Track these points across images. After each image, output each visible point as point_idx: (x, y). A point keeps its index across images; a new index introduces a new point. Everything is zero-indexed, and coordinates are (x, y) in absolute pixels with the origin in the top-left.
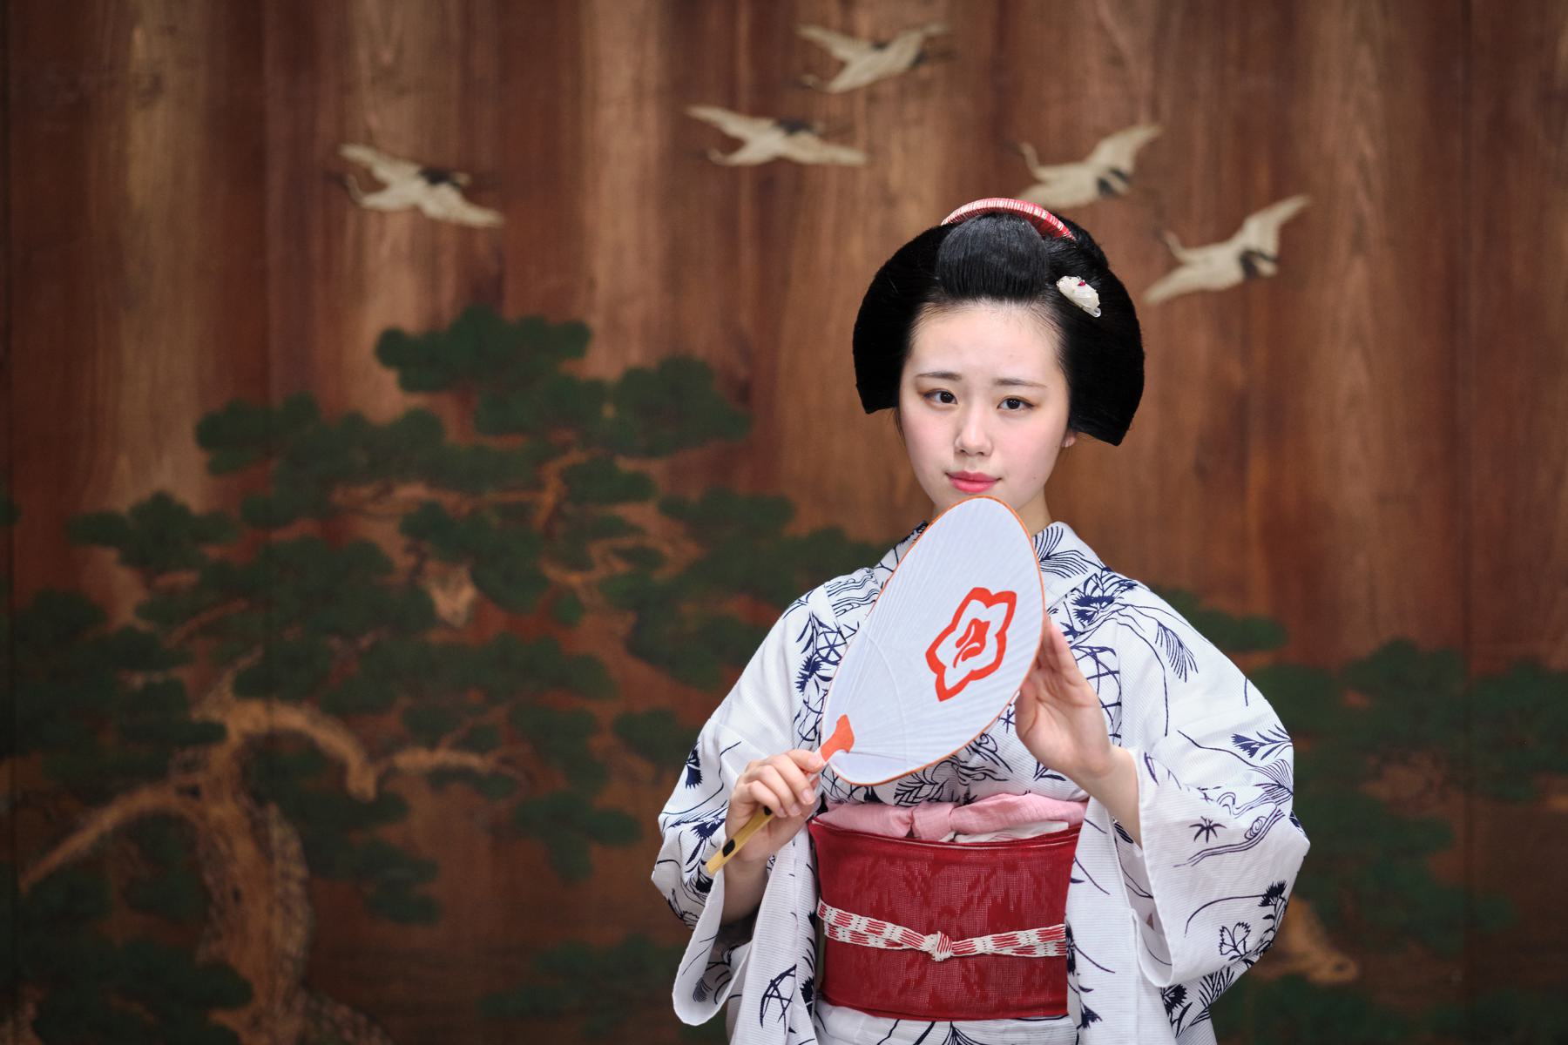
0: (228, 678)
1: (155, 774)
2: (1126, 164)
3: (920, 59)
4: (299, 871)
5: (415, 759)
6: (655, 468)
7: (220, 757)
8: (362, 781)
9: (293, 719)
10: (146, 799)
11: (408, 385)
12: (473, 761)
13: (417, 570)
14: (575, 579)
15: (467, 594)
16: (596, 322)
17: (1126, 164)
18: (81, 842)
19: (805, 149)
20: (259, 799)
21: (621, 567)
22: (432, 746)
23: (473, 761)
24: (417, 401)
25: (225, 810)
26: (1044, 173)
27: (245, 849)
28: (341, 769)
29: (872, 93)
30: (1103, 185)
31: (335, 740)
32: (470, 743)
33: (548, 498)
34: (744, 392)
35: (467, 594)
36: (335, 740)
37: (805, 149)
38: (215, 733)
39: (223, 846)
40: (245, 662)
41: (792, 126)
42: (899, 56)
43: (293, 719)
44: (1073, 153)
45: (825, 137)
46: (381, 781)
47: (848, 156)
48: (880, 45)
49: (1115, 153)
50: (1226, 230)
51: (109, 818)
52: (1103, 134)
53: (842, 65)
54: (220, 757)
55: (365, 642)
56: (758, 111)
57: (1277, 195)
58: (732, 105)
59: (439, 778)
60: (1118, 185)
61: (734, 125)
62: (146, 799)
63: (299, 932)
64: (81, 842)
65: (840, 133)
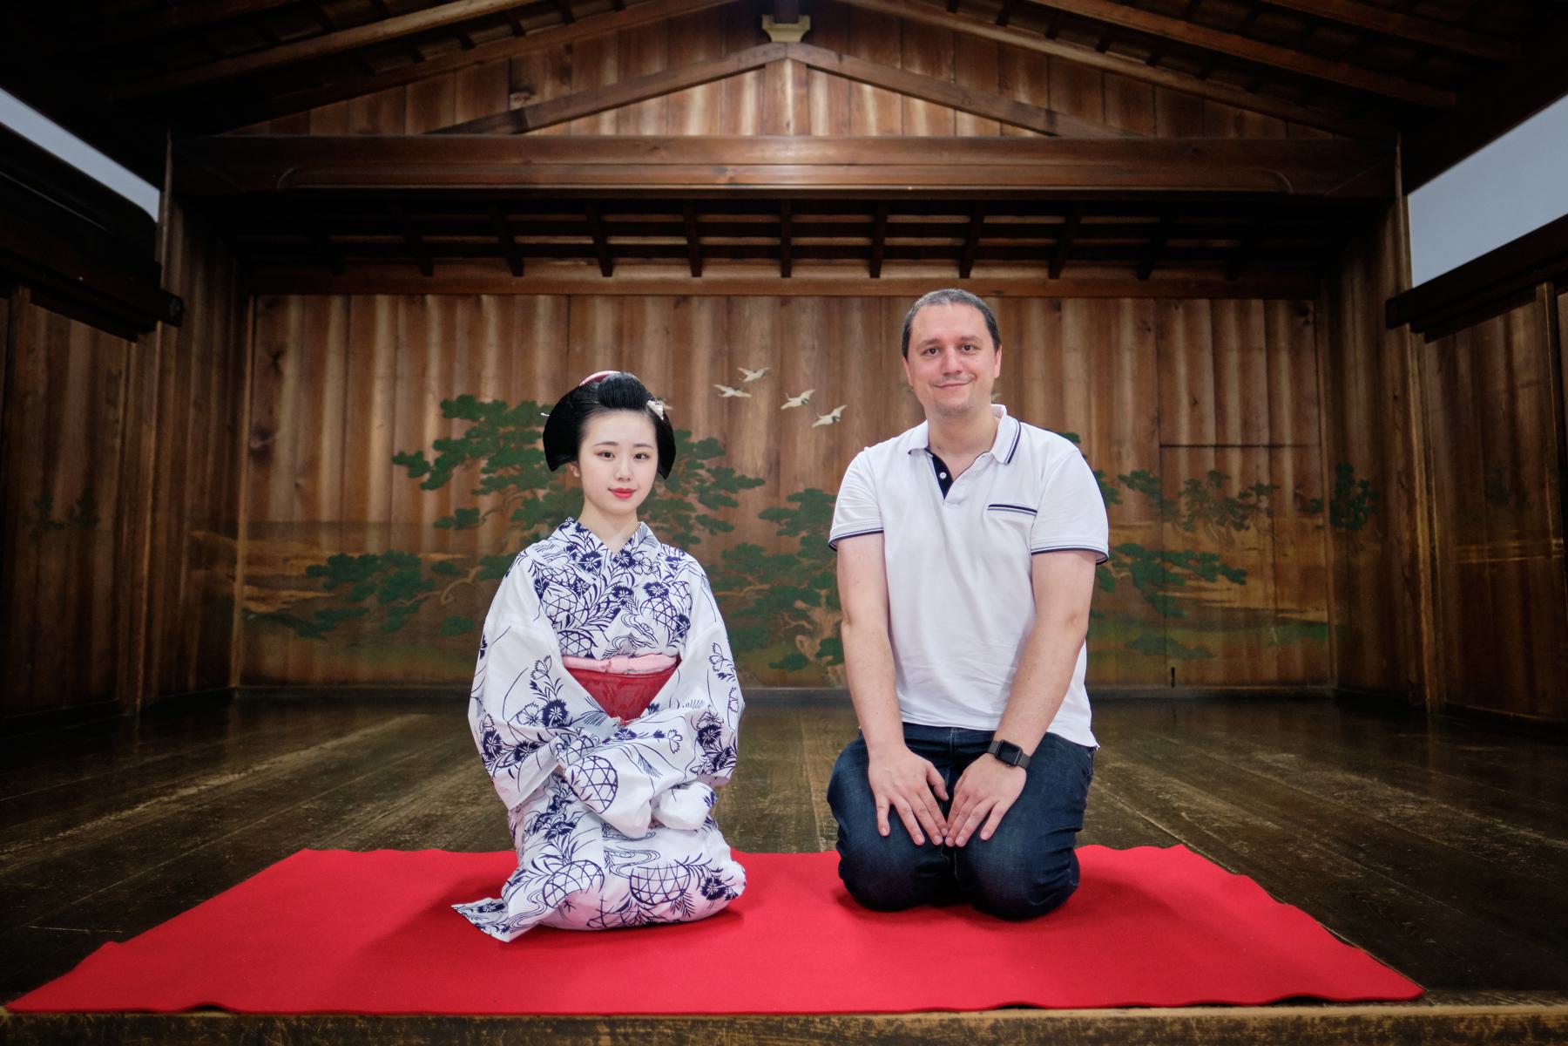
2: (807, 398)
3: (764, 375)
6: (705, 462)
12: (664, 525)
14: (687, 486)
16: (693, 431)
17: (807, 398)
19: (739, 394)
21: (697, 483)
23: (664, 525)
26: (790, 399)
29: (753, 382)
30: (803, 402)
34: (725, 446)
37: (739, 394)
41: (736, 389)
42: (759, 374)
44: (797, 395)
45: (743, 391)
47: (747, 395)
48: (755, 372)
49: (805, 395)
50: (829, 413)
52: (803, 391)
53: (746, 376)
56: (728, 386)
57: (840, 405)
58: (723, 384)
60: (806, 402)
61: (723, 388)
65: (746, 390)
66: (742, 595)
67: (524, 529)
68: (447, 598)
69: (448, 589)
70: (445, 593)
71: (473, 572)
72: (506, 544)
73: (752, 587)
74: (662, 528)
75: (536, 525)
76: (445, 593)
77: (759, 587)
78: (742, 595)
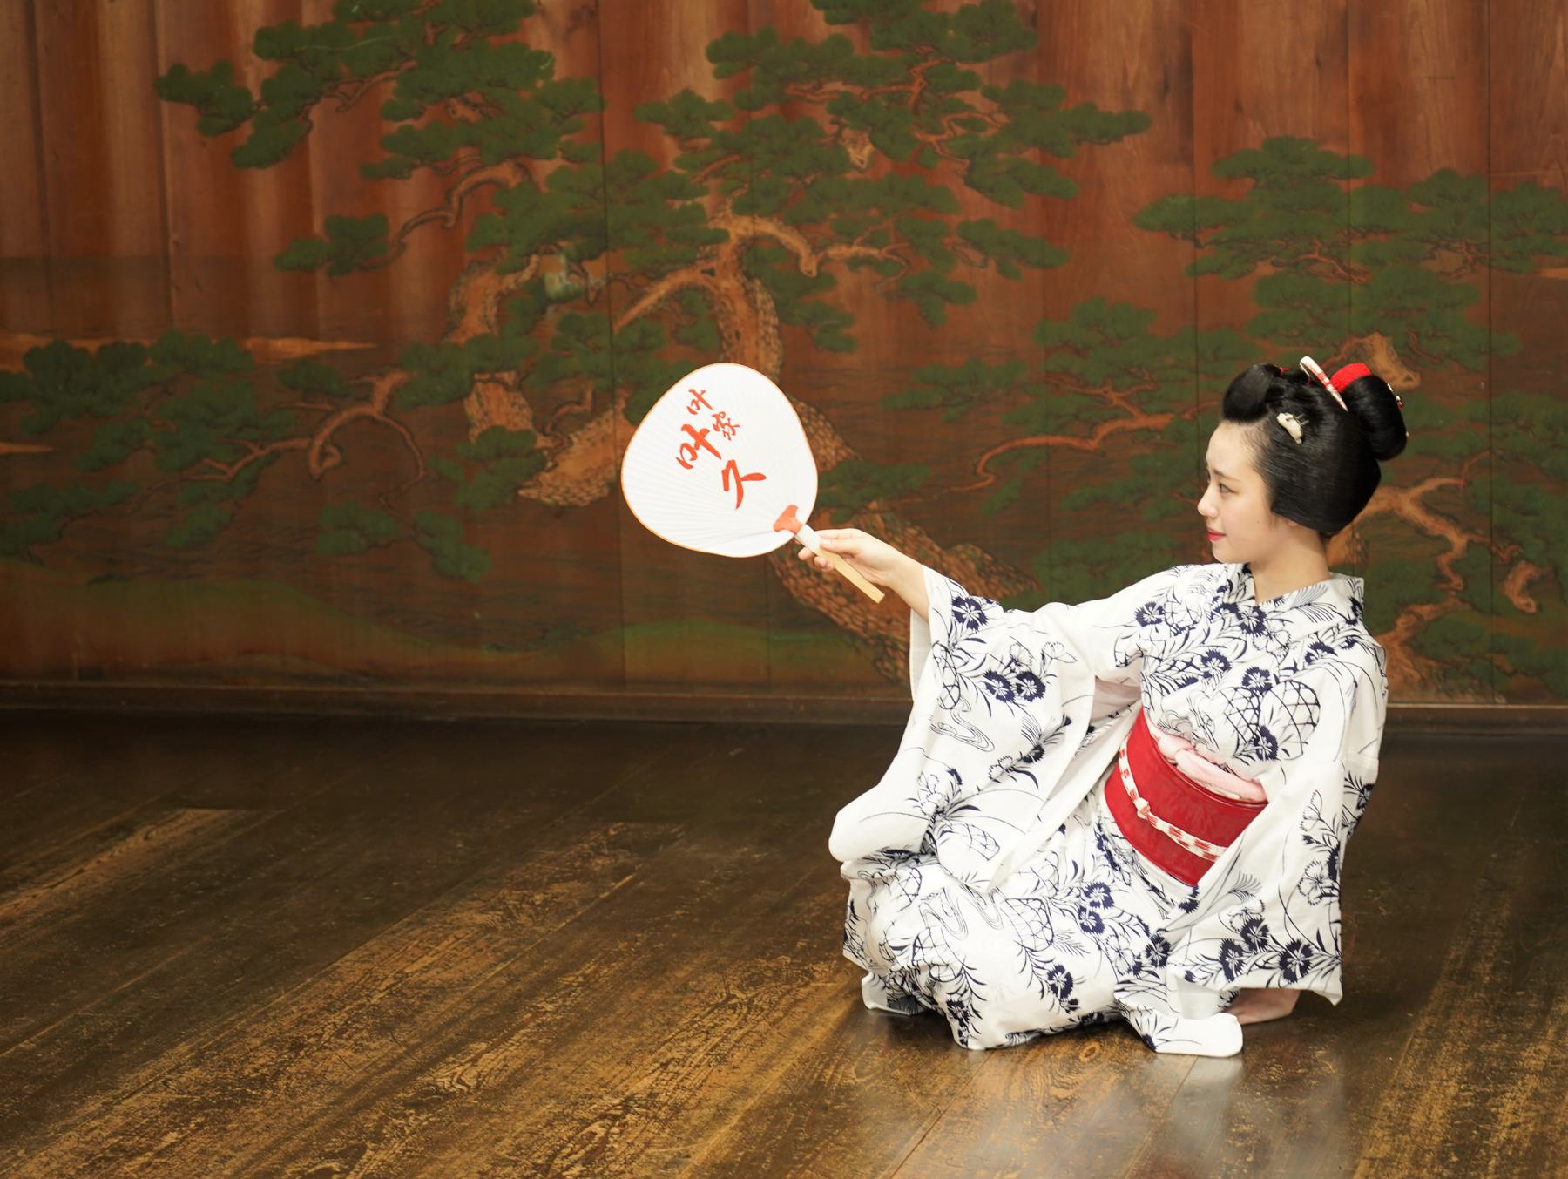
0: (730, 202)
1: (690, 263)
4: (774, 321)
5: (837, 252)
6: (980, 69)
7: (726, 250)
8: (809, 266)
9: (768, 227)
10: (684, 277)
11: (831, 21)
12: (874, 252)
13: (838, 135)
14: (932, 139)
15: (869, 148)
18: (647, 303)
20: (749, 276)
21: (960, 131)
22: (850, 244)
23: (874, 252)
24: (837, 29)
25: (729, 283)
27: (742, 307)
28: (797, 258)
31: (793, 241)
32: (870, 242)
33: (916, 89)
35: (869, 148)
36: (793, 241)
38: (721, 237)
39: (728, 303)
40: (738, 193)
43: (768, 227)
46: (820, 265)
51: (663, 288)
54: (726, 250)
55: (808, 181)
59: (855, 263)
62: (684, 277)
63: (775, 357)
64: (647, 303)
66: (1092, 444)
67: (502, 272)
68: (323, 455)
69: (326, 432)
70: (318, 443)
71: (383, 387)
72: (462, 311)
73: (1119, 424)
74: (868, 261)
75: (534, 258)
76: (318, 443)
77: (1142, 422)
78: (1092, 444)
